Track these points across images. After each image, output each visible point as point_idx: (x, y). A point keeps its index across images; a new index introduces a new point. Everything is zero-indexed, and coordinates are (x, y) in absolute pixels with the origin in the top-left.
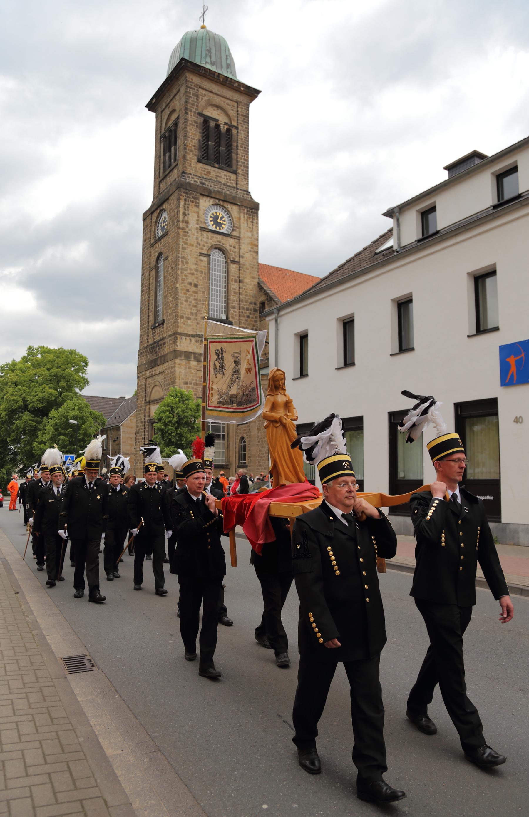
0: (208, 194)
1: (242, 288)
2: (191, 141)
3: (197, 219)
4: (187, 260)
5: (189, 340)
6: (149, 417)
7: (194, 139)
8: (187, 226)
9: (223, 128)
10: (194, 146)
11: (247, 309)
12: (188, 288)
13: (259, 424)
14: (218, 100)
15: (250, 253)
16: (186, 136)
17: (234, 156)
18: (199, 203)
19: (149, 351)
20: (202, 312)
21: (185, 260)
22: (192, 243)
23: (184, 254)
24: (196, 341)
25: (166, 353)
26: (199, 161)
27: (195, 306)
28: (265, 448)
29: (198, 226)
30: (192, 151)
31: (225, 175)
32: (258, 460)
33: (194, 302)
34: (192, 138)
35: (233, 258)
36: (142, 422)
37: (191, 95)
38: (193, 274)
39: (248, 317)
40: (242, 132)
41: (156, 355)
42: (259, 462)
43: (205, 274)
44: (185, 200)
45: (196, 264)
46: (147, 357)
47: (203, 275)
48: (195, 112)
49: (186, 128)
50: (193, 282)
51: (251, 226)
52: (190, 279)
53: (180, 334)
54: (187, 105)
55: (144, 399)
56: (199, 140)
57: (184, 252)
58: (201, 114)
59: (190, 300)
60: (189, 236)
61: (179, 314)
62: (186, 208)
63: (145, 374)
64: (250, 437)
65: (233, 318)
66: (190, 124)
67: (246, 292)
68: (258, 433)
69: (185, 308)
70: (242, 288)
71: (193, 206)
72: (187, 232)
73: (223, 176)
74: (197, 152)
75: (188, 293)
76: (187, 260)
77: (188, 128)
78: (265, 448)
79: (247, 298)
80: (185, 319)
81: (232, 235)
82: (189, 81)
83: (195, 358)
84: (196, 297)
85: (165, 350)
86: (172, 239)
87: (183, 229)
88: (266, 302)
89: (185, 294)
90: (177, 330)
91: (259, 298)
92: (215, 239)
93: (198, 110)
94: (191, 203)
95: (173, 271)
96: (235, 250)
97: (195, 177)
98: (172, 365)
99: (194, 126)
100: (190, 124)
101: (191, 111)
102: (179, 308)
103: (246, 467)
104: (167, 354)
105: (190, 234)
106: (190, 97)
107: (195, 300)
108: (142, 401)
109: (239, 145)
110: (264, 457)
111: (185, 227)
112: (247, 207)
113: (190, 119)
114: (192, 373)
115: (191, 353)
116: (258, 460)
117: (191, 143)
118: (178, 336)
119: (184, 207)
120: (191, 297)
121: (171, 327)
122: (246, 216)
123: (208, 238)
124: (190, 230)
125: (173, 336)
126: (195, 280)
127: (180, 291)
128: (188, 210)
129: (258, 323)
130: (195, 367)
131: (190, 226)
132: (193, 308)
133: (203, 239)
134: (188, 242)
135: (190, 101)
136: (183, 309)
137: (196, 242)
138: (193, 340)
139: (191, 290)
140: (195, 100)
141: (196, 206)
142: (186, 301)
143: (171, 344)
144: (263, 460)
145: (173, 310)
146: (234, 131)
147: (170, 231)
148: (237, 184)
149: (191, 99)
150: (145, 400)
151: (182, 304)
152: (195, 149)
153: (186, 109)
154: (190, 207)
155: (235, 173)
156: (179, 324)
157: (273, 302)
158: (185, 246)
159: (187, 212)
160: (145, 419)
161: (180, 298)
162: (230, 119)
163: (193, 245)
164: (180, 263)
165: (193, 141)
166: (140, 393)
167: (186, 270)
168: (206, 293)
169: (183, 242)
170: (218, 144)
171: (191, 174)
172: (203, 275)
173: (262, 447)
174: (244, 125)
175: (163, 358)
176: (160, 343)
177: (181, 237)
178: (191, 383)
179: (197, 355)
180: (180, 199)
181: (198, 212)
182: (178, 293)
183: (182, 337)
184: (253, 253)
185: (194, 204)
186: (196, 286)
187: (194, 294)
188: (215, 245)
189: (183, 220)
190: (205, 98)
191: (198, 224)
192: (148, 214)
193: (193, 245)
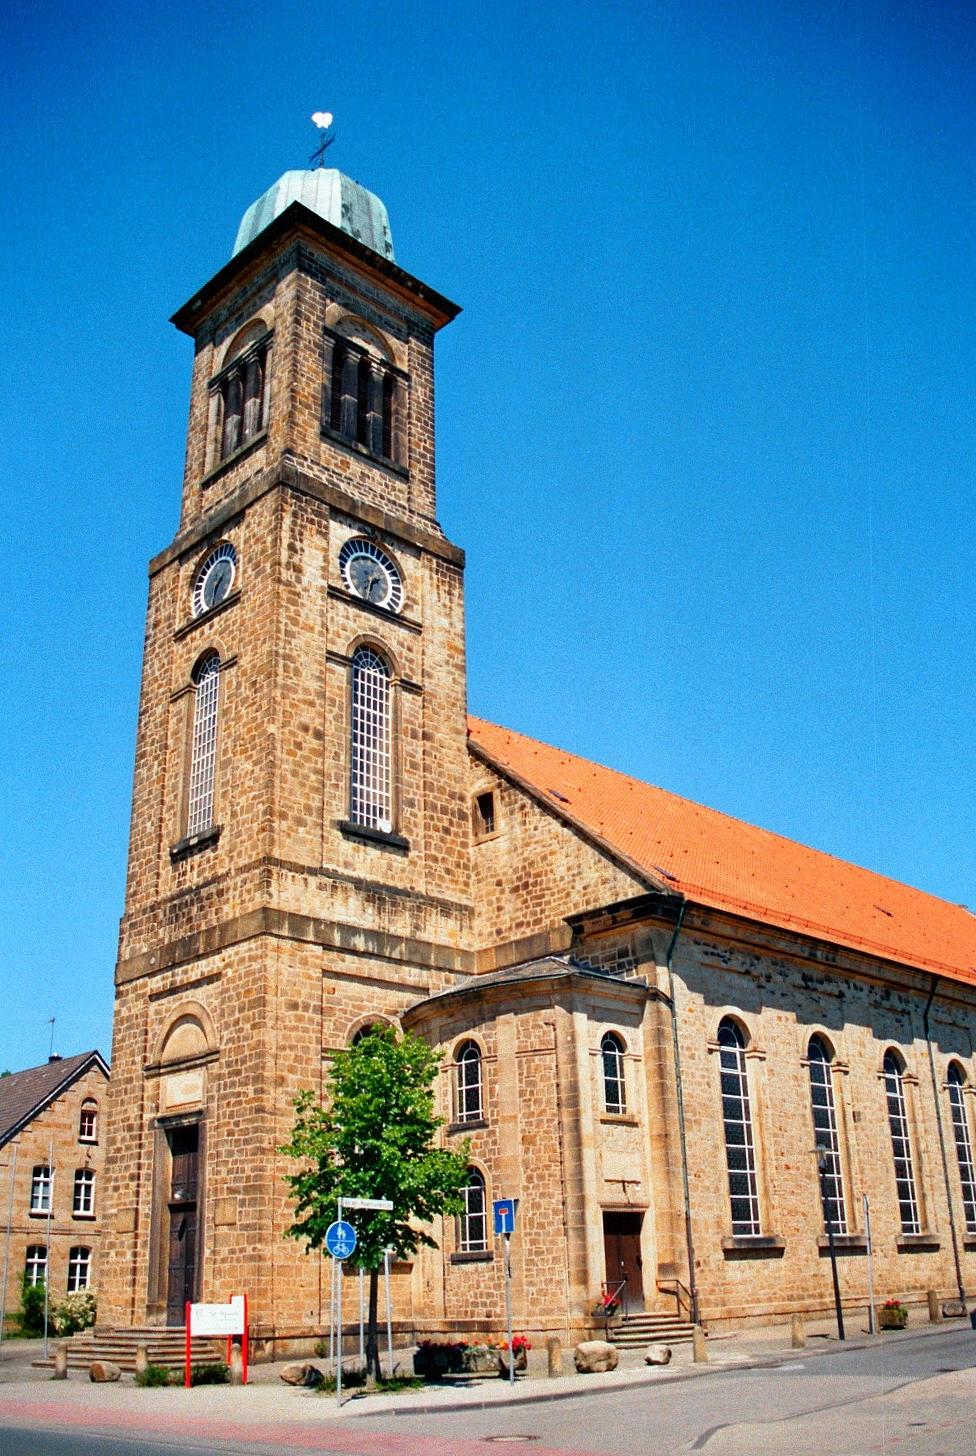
1: (430, 754)
2: (308, 385)
3: (323, 564)
4: (298, 664)
5: (302, 883)
6: (157, 1109)
7: (314, 382)
8: (299, 581)
9: (378, 372)
10: (313, 397)
11: (444, 811)
12: (299, 740)
13: (529, 1124)
15: (446, 668)
16: (295, 371)
18: (326, 527)
19: (161, 916)
20: (334, 808)
21: (292, 665)
22: (311, 622)
23: (291, 649)
24: (321, 887)
25: (231, 917)
27: (316, 790)
28: (551, 1196)
29: (324, 583)
30: (308, 407)
32: (530, 1234)
33: (313, 777)
34: (308, 378)
35: (406, 675)
36: (130, 1128)
37: (309, 287)
38: (311, 704)
39: (447, 831)
40: (420, 388)
41: (191, 929)
42: (533, 1242)
43: (341, 708)
44: (295, 515)
45: (319, 679)
46: (157, 933)
47: (336, 710)
48: (316, 324)
49: (296, 353)
50: (311, 726)
51: (448, 603)
52: (308, 716)
53: (280, 863)
54: (299, 305)
55: (138, 1059)
56: (324, 387)
57: (290, 643)
59: (306, 771)
60: (303, 605)
61: (277, 808)
62: (297, 534)
63: (145, 985)
64: (497, 1167)
65: (410, 831)
66: (305, 346)
67: (440, 766)
68: (526, 1151)
69: (291, 792)
70: (430, 754)
71: (314, 531)
72: (298, 595)
74: (317, 411)
75: (299, 753)
76: (298, 664)
77: (301, 354)
79: (442, 780)
80: (290, 822)
81: (404, 619)
82: (304, 256)
83: (317, 933)
84: (319, 766)
85: (226, 908)
86: (253, 610)
87: (288, 584)
88: (497, 793)
89: (290, 753)
90: (271, 850)
91: (472, 784)
93: (323, 319)
94: (309, 526)
95: (256, 692)
96: (411, 655)
97: (315, 468)
98: (253, 953)
99: (314, 352)
100: (305, 346)
101: (308, 320)
102: (277, 791)
104: (235, 920)
105: (304, 600)
106: (306, 290)
107: (316, 772)
108: (133, 1063)
110: (551, 1224)
111: (293, 580)
112: (437, 556)
113: (305, 336)
114: (310, 977)
115: (308, 918)
116: (530, 1234)
117: (307, 389)
118: (275, 870)
119: (292, 531)
120: (307, 765)
121: (248, 844)
122: (435, 576)
123: (347, 618)
124: (305, 590)
125: (255, 868)
126: (318, 721)
127: (278, 746)
128: (301, 541)
129: (471, 850)
130: (318, 961)
131: (305, 580)
132: (312, 795)
133: (336, 618)
134: (301, 619)
136: (286, 794)
137: (319, 623)
138: (313, 881)
140: (318, 298)
141: (319, 532)
142: (295, 773)
143: (249, 891)
144: (548, 1234)
145: (254, 798)
147: (246, 592)
148: (409, 500)
149: (308, 295)
150: (145, 1059)
151: (283, 779)
152: (316, 404)
153: (297, 312)
154: (306, 534)
156: (276, 837)
158: (295, 629)
159: (298, 545)
160: (141, 1117)
161: (278, 762)
164: (280, 670)
165: (313, 385)
166: (123, 1040)
167: (296, 692)
168: (342, 758)
169: (288, 617)
170: (363, 406)
171: (306, 459)
172: (336, 710)
173: (542, 1195)
174: (424, 373)
175: (218, 933)
176: (204, 892)
177: (284, 603)
178: (306, 1008)
179: (323, 927)
180: (283, 510)
181: (326, 550)
182: (274, 748)
183: (284, 871)
184: (453, 670)
185: (315, 527)
186: (319, 735)
187: (314, 758)
188: (364, 635)
189: (288, 563)
191: (323, 577)
192: (168, 558)
193: (311, 629)
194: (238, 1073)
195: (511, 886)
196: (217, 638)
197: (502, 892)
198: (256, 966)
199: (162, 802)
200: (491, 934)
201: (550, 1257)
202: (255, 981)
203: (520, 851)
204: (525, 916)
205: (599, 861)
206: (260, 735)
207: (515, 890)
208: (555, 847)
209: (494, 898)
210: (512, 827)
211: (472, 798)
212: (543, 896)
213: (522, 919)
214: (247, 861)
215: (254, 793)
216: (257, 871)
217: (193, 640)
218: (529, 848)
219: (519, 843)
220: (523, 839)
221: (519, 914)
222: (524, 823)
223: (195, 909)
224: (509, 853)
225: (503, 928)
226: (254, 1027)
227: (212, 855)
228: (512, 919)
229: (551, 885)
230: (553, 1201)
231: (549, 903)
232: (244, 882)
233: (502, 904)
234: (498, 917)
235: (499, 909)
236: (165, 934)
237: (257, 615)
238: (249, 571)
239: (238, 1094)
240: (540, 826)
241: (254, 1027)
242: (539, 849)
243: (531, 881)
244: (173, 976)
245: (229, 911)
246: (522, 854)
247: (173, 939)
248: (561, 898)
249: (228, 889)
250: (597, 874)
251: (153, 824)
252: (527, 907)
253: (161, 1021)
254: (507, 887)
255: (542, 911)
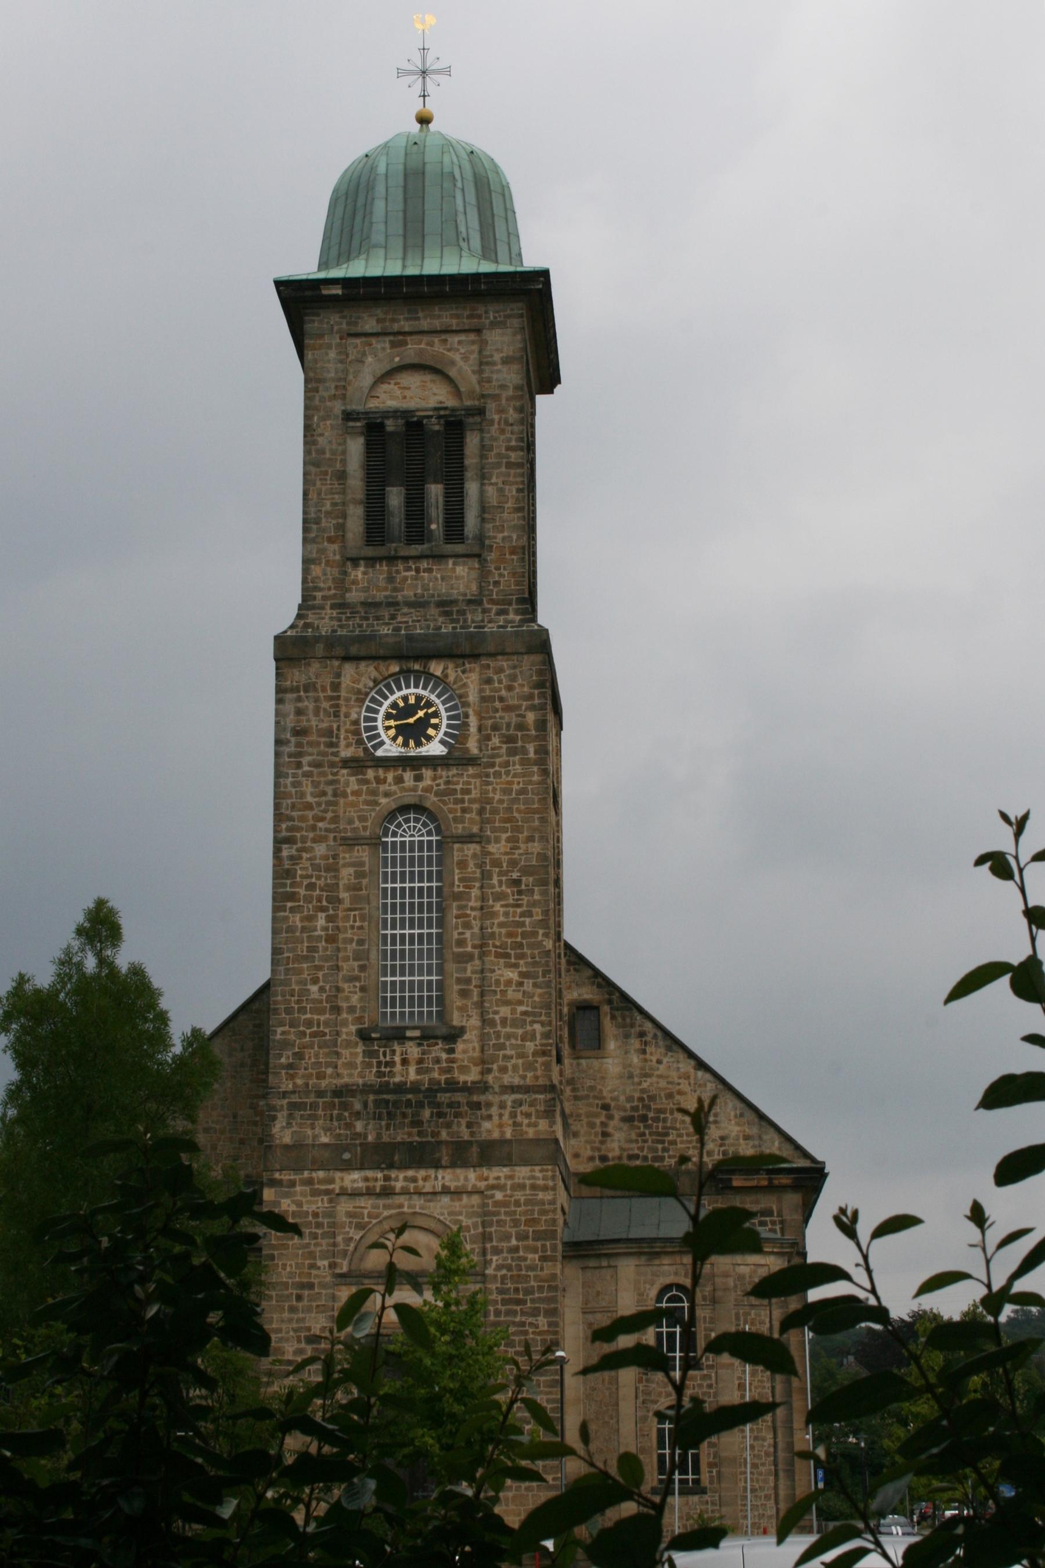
28: (764, 1439)
78: (764, 1439)
86: (506, 791)
88: (606, 1008)
95: (520, 893)
103: (703, 1491)
108: (313, 1266)
110: (763, 1464)
125: (541, 1093)
143: (528, 1115)
144: (761, 1474)
150: (333, 1266)
157: (636, 1014)
194: (519, 1302)
195: (622, 1114)
196: (434, 798)
197: (610, 1117)
198: (541, 1195)
199: (338, 968)
200: (591, 1159)
201: (763, 1494)
202: (543, 1212)
203: (636, 1080)
204: (642, 1149)
205: (742, 1115)
206: (531, 946)
207: (628, 1119)
208: (684, 1086)
209: (598, 1121)
210: (626, 1053)
211: (569, 1005)
212: (667, 1134)
213: (636, 1152)
214: (517, 1081)
215: (523, 1008)
216: (542, 1097)
217: (379, 781)
218: (649, 1080)
219: (637, 1072)
220: (642, 1069)
221: (634, 1145)
222: (644, 1052)
223: (427, 1113)
224: (621, 1077)
225: (610, 1155)
226: (544, 1259)
227: (444, 1056)
228: (621, 1149)
229: (678, 1125)
230: (766, 1444)
231: (672, 1143)
232: (519, 1103)
233: (610, 1130)
234: (602, 1142)
235: (605, 1134)
236: (368, 1130)
237: (515, 801)
238: (496, 741)
239: (523, 1324)
240: (665, 1060)
241: (544, 1259)
242: (663, 1084)
243: (651, 1115)
244: (387, 1178)
245: (489, 1129)
246: (640, 1083)
247: (385, 1139)
248: (690, 1142)
249: (489, 1105)
250: (737, 1128)
251: (322, 989)
252: (645, 1141)
253: (360, 1226)
254: (618, 1115)
255: (665, 1150)
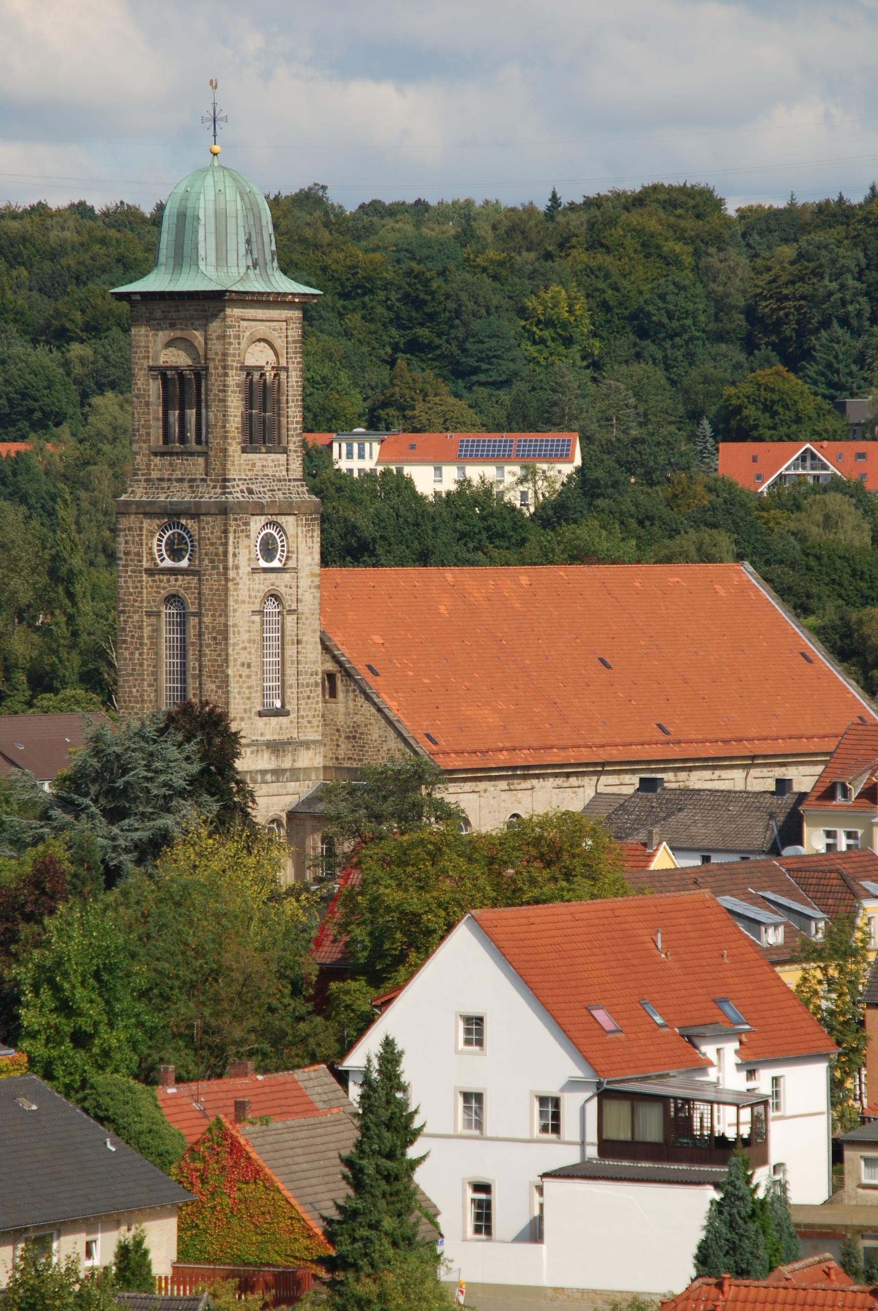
0: (259, 509)
8: (238, 574)
9: (269, 375)
14: (261, 329)
17: (284, 420)
24: (252, 753)
26: (244, 451)
31: (273, 461)
39: (309, 697)
44: (235, 532)
58: (243, 368)
73: (271, 464)
89: (238, 682)
92: (268, 582)
97: (240, 483)
109: (290, 398)
115: (247, 772)
131: (240, 572)
135: (231, 351)
139: (244, 674)
142: (239, 693)
146: (283, 375)
148: (287, 470)
155: (285, 451)
162: (276, 354)
163: (244, 602)
190: (247, 334)
193: (244, 602)
